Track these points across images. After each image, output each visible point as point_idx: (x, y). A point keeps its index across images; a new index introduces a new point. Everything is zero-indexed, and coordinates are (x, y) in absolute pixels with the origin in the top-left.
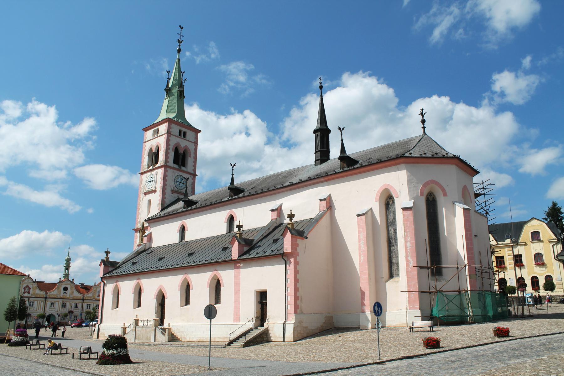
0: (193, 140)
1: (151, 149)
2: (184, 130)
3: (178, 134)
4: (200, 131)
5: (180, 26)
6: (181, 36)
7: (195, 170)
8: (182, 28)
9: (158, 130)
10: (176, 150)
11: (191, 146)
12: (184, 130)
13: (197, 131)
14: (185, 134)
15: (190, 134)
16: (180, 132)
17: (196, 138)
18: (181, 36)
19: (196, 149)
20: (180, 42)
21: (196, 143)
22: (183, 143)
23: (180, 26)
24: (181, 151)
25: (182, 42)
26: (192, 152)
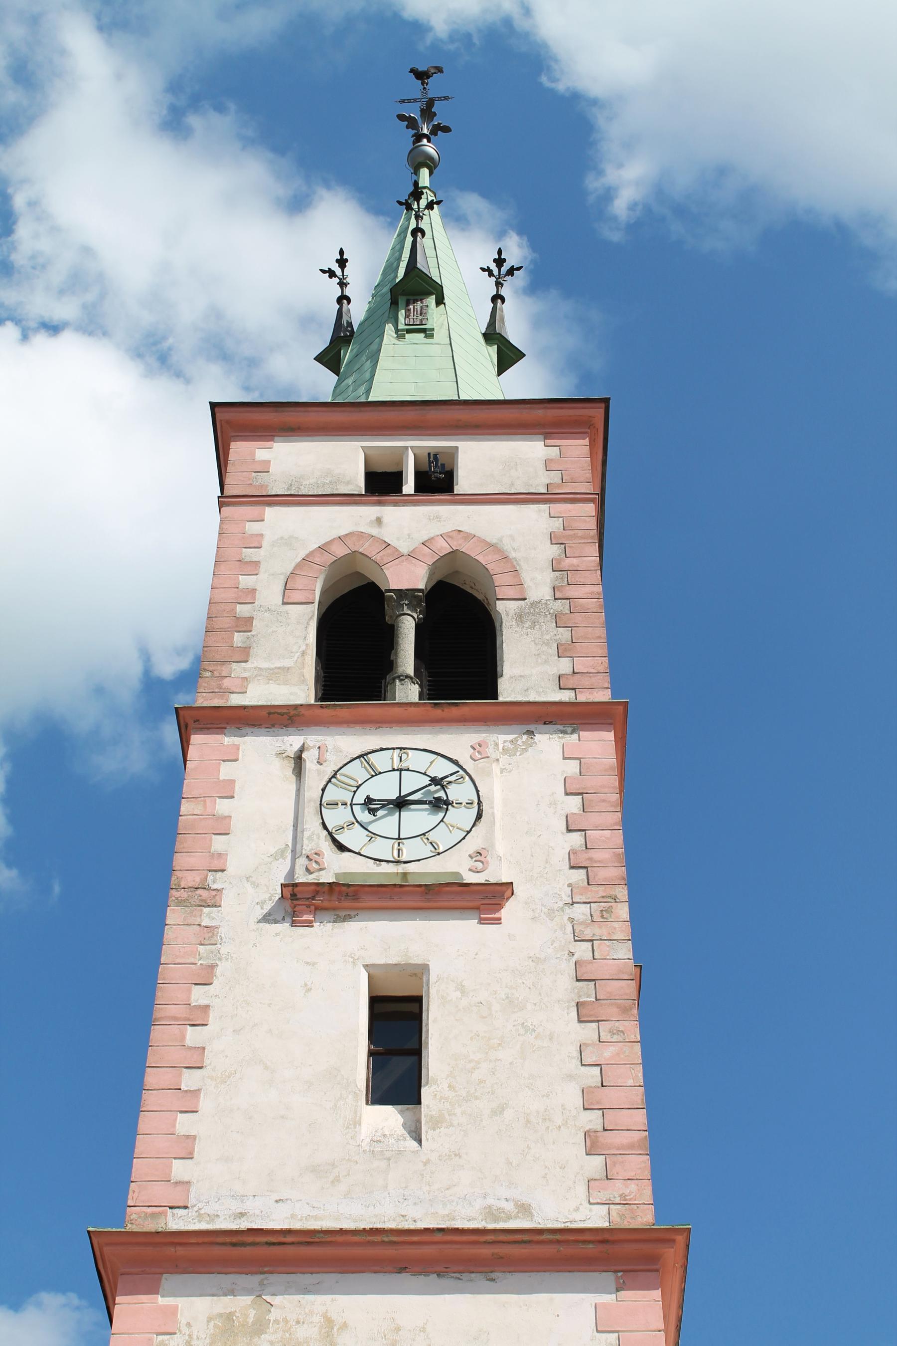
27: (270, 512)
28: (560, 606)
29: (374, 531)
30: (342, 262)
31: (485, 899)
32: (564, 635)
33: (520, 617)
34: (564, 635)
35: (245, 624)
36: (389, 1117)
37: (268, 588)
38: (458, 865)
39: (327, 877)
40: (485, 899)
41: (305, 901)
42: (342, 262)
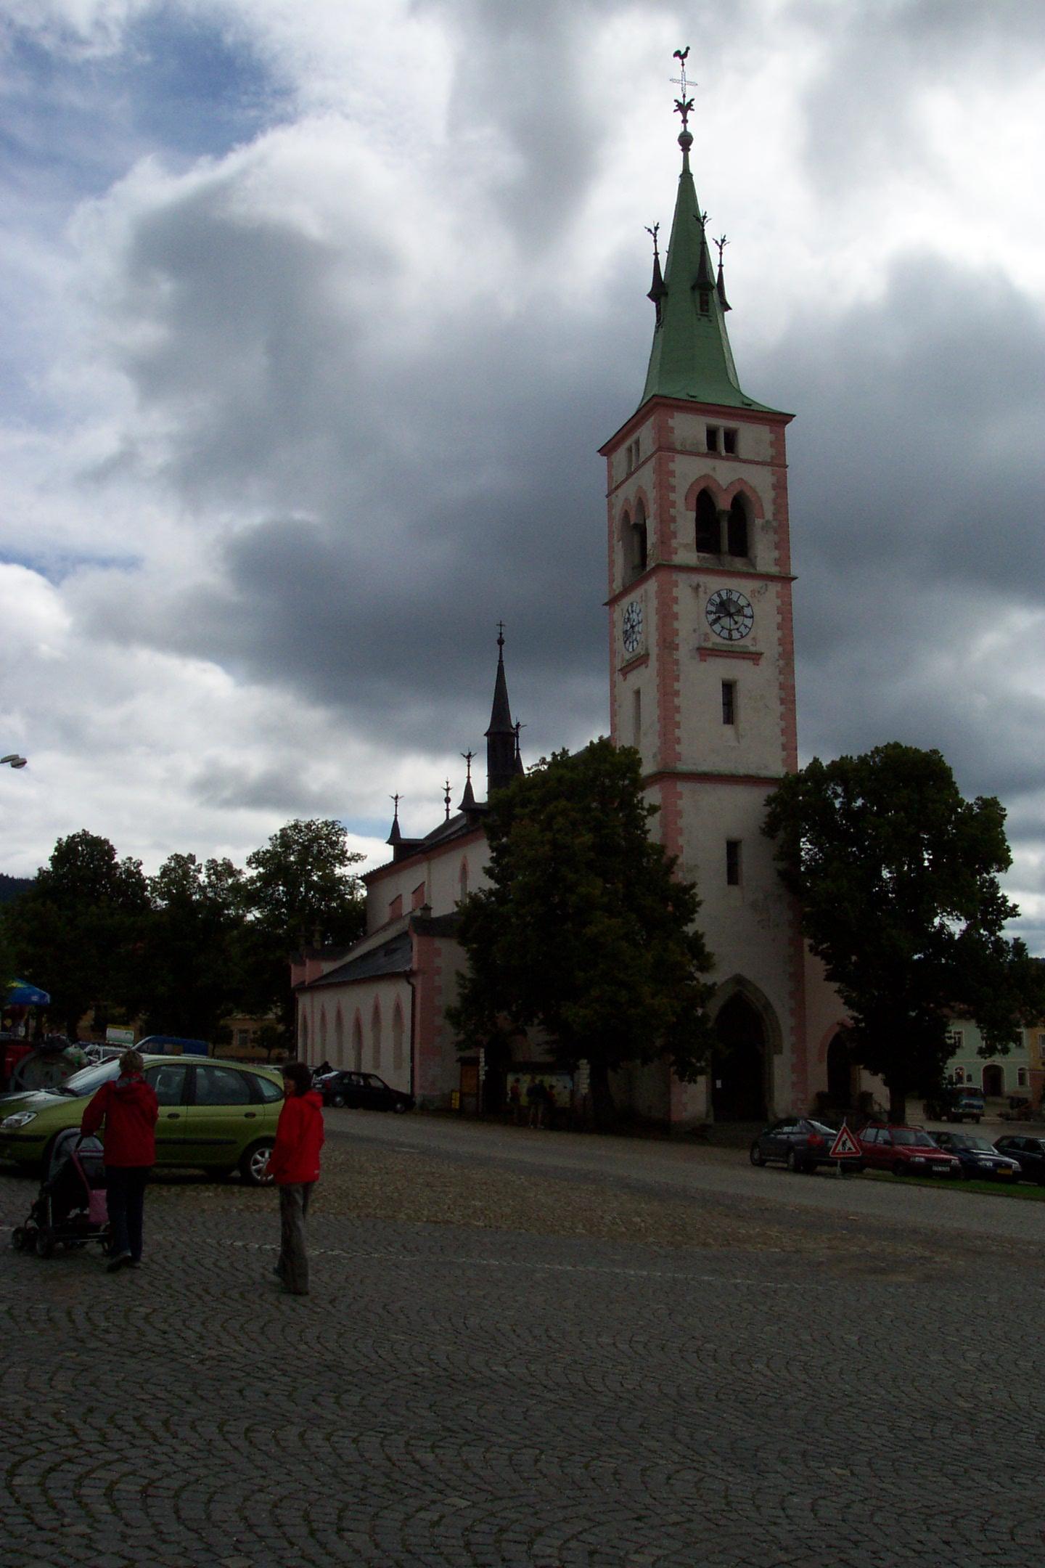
0: (767, 453)
1: (626, 515)
2: (722, 423)
3: (704, 448)
4: (789, 417)
5: (677, 54)
6: (684, 82)
7: (784, 560)
8: (683, 56)
9: (637, 442)
10: (704, 501)
11: (759, 480)
12: (722, 423)
13: (780, 420)
14: (731, 439)
15: (751, 438)
16: (712, 434)
17: (779, 444)
18: (684, 82)
19: (781, 487)
20: (684, 108)
21: (778, 462)
22: (724, 474)
23: (677, 54)
24: (724, 503)
25: (690, 104)
26: (766, 496)
27: (679, 458)
28: (775, 524)
29: (711, 473)
30: (656, 228)
31: (755, 657)
32: (776, 538)
33: (763, 528)
34: (776, 538)
35: (673, 520)
36: (728, 730)
37: (678, 497)
38: (747, 642)
39: (709, 645)
40: (755, 657)
41: (705, 653)
42: (656, 228)
